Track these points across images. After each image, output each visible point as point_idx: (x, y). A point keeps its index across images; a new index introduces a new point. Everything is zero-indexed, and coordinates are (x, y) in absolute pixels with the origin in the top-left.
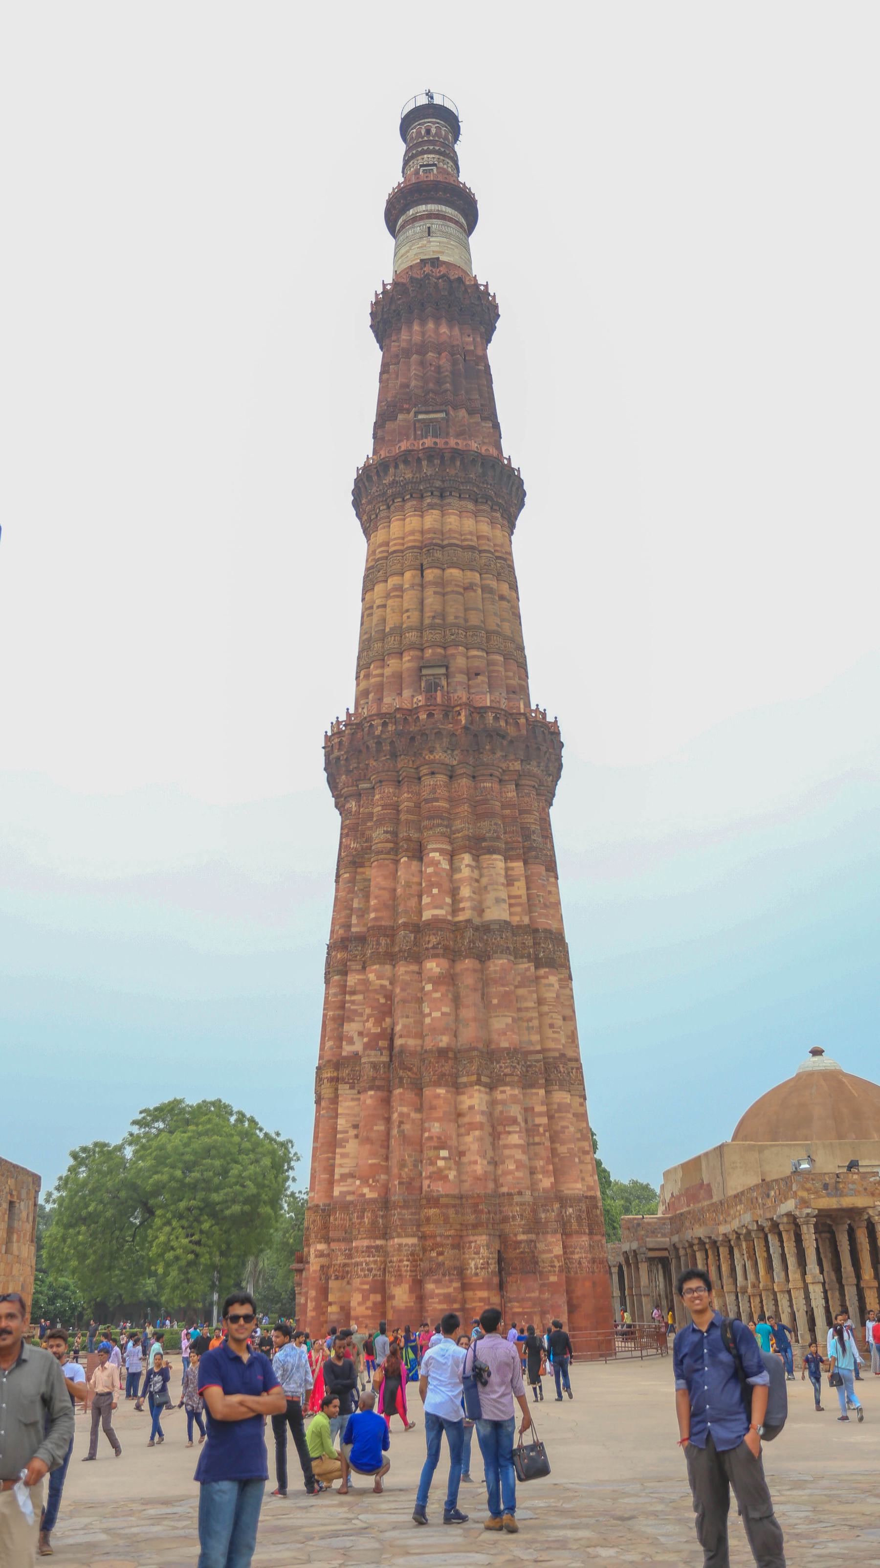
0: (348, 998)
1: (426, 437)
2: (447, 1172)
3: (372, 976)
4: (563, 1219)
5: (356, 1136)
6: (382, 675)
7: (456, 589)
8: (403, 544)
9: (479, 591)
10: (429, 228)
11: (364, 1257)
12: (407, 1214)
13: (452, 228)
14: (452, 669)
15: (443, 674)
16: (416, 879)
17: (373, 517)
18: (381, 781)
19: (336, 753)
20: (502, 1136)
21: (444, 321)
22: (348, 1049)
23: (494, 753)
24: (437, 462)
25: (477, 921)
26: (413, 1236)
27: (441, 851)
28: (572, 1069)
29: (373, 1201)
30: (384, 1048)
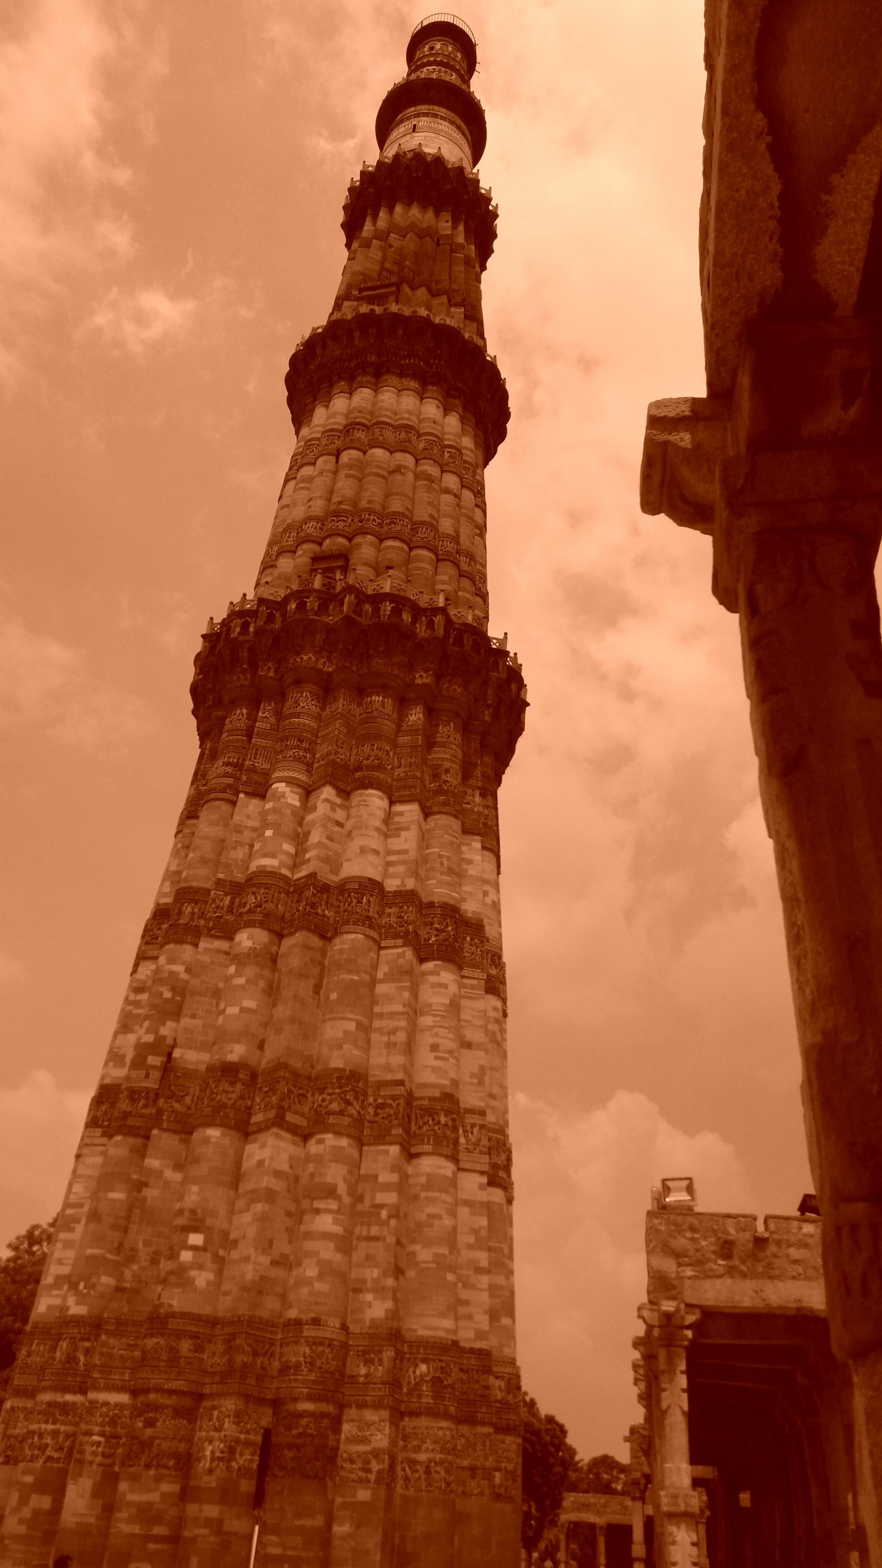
2: (193, 1273)
3: (162, 960)
4: (409, 1383)
7: (375, 470)
9: (410, 476)
10: (415, 125)
11: (39, 1422)
12: (116, 1345)
13: (445, 126)
15: (340, 567)
16: (251, 823)
20: (306, 1218)
24: (372, 331)
26: (120, 1389)
27: (289, 781)
28: (473, 1126)
29: (78, 1321)
30: (154, 1067)
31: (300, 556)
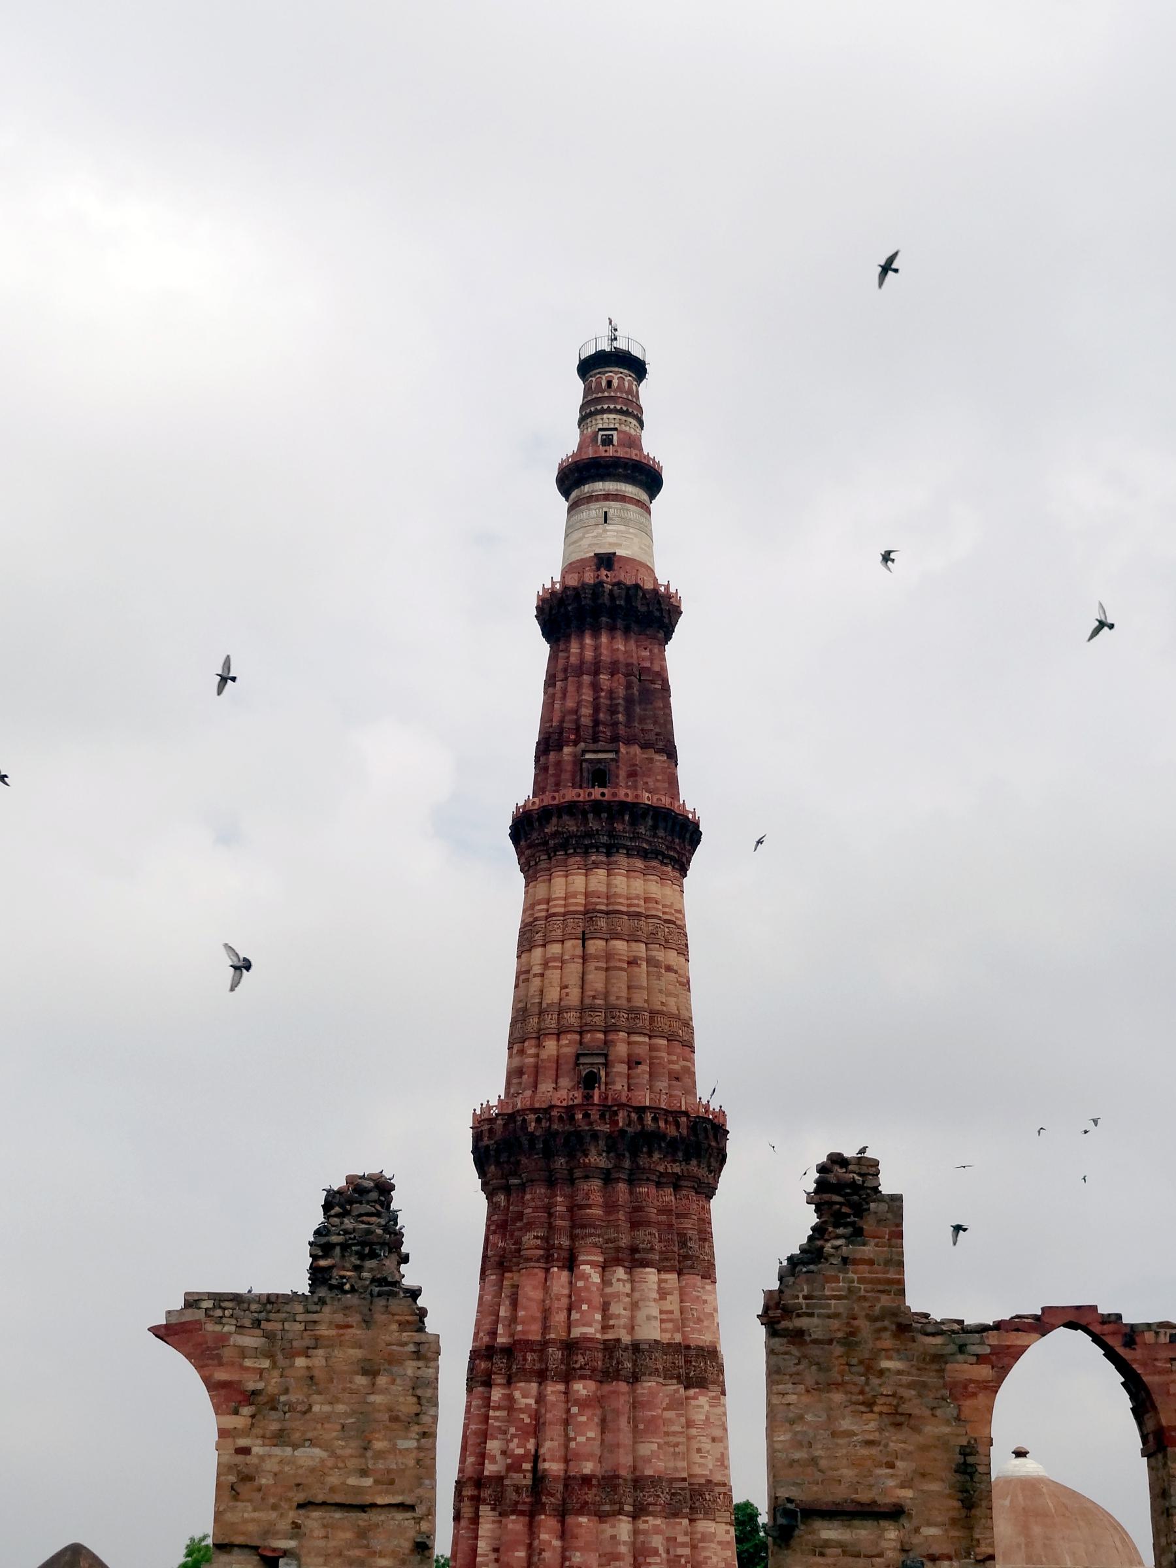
0: (491, 1413)
1: (593, 787)
3: (517, 1394)
5: (497, 1560)
6: (537, 1055)
8: (565, 906)
9: (645, 963)
13: (633, 511)
14: (610, 1058)
16: (566, 1292)
17: (532, 863)
18: (532, 1181)
19: (486, 1141)
21: (619, 634)
22: (490, 1469)
23: (651, 1156)
25: (626, 1339)
27: (592, 1264)
31: (567, 1046)
